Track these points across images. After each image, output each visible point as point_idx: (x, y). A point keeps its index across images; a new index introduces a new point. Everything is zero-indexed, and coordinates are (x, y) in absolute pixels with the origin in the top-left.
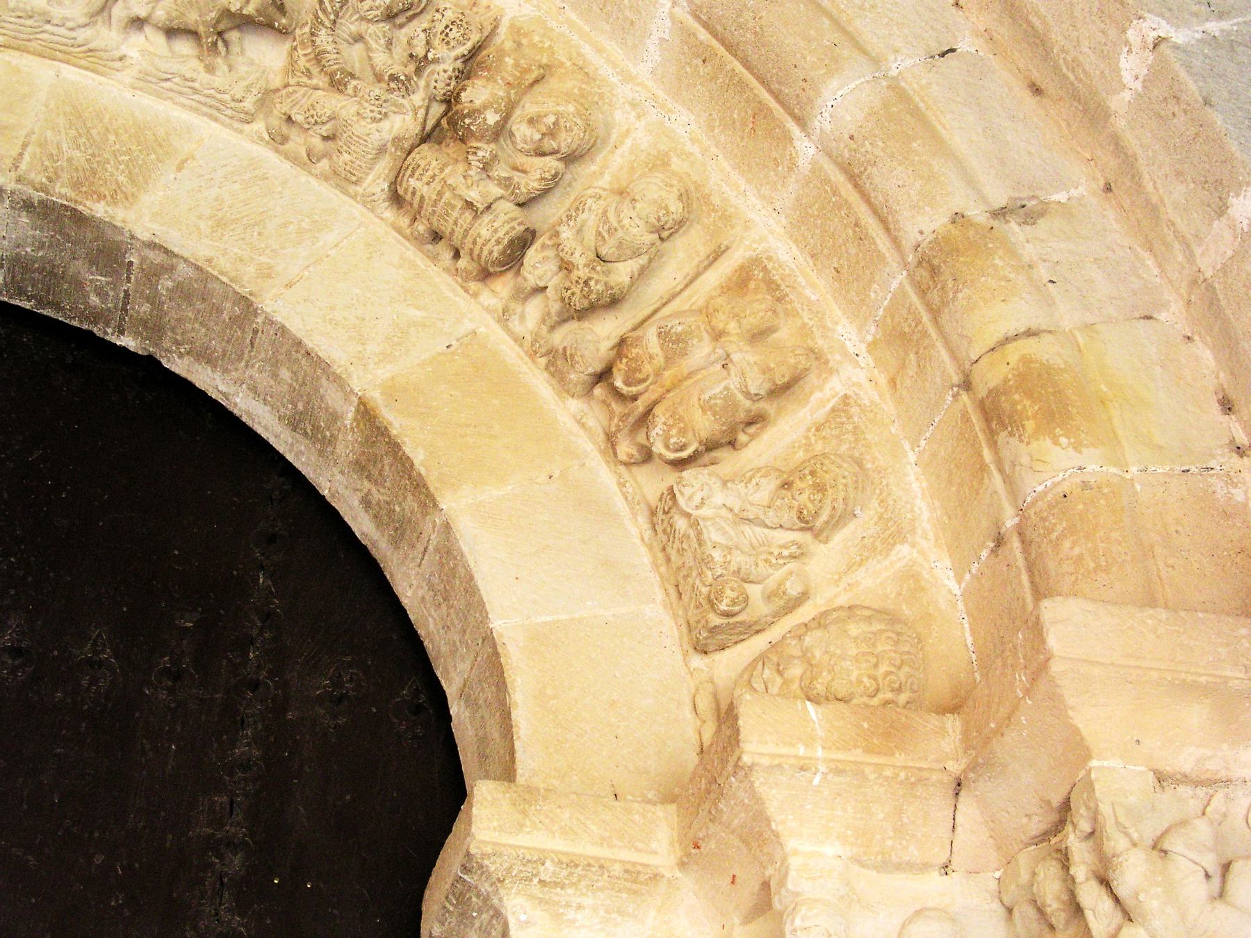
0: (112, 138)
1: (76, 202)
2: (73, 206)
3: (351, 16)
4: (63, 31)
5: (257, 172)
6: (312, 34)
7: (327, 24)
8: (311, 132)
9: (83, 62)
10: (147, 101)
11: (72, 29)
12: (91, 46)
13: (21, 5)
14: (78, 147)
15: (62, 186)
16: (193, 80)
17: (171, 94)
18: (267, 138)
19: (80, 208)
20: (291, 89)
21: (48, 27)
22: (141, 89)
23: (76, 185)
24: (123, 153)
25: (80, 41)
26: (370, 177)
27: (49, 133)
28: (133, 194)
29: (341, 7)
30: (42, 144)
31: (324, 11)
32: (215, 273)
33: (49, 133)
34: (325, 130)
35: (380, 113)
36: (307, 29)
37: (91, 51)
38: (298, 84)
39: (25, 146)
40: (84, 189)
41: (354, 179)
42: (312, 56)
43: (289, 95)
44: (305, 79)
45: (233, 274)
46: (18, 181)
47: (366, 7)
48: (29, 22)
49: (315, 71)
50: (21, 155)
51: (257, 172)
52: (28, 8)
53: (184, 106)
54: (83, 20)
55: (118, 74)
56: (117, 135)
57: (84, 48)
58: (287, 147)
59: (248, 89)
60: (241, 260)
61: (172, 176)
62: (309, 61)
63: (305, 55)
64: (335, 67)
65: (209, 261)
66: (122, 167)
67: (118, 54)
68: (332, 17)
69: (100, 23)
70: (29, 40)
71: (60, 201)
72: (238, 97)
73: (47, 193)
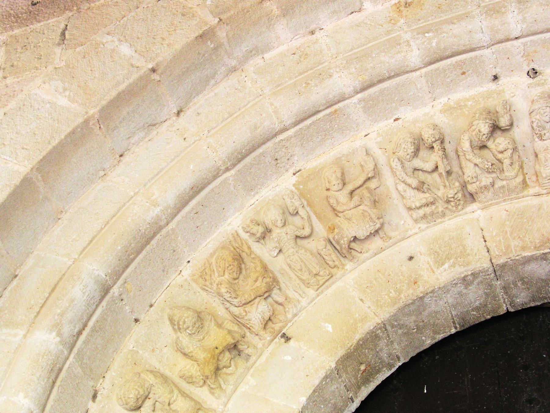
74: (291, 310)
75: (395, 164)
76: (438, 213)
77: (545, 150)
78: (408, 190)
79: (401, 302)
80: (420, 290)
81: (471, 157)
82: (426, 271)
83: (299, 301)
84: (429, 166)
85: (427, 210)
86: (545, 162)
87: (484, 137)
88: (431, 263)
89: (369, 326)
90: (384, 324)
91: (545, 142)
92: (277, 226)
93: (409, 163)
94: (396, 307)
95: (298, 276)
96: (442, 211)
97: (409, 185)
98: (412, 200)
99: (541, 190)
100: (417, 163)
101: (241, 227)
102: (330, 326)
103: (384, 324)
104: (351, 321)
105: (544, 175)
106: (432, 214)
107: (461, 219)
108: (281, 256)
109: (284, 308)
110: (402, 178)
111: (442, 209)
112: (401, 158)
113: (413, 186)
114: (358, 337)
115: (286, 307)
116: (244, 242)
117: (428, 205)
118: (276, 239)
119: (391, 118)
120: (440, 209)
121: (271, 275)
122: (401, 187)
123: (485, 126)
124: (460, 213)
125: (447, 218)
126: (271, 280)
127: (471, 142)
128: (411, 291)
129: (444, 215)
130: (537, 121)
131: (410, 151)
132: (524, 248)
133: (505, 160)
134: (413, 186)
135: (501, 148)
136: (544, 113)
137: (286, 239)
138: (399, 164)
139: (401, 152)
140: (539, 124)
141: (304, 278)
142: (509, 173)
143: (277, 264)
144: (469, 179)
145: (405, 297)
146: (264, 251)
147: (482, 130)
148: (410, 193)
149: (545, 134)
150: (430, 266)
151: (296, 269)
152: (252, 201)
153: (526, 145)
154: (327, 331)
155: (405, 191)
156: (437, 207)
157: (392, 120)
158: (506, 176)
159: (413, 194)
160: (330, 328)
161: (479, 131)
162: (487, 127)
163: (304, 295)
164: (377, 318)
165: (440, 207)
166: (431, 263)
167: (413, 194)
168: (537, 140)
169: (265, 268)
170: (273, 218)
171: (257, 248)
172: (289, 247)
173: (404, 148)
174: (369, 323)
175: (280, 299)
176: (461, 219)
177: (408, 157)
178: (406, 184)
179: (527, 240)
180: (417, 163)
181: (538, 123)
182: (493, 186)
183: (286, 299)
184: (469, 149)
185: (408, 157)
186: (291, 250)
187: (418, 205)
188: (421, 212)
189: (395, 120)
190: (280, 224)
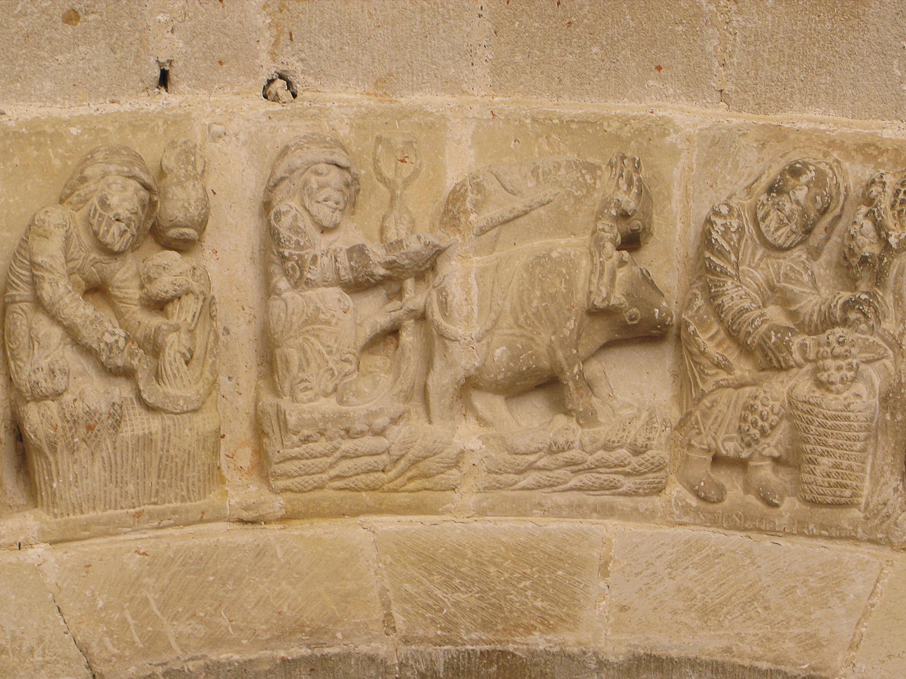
0: (492, 570)
1: (500, 642)
2: (499, 647)
3: (753, 254)
4: (368, 442)
5: (704, 553)
6: (712, 298)
7: (730, 269)
8: (752, 463)
9: (402, 498)
10: (508, 524)
11: (381, 433)
12: (410, 456)
13: (306, 416)
14: (456, 589)
15: (468, 631)
16: (569, 446)
17: (537, 495)
18: (693, 502)
19: (511, 647)
20: (706, 402)
21: (347, 445)
22: (493, 510)
23: (486, 625)
24: (519, 580)
25: (395, 451)
26: (867, 484)
27: (407, 586)
28: (568, 615)
29: (739, 240)
30: (408, 599)
31: (721, 253)
32: (747, 662)
33: (407, 586)
34: (772, 446)
35: (850, 367)
36: (699, 302)
37: (414, 463)
38: (719, 386)
39: (386, 605)
40: (500, 627)
41: (848, 493)
42: (722, 334)
43: (705, 415)
44: (723, 375)
45: (771, 655)
46: (406, 641)
47: (773, 225)
48: (321, 445)
49: (732, 355)
50: (389, 615)
51: (704, 553)
52: (317, 416)
53: (557, 511)
54: (399, 406)
55: (455, 496)
56: (495, 564)
57: (402, 463)
58: (726, 502)
59: (649, 424)
60: (769, 639)
61: (602, 584)
62: (718, 345)
63: (712, 338)
64: (765, 326)
65: (728, 650)
66: (529, 593)
67: (452, 451)
68: (733, 258)
69: (414, 416)
70: (321, 488)
71: (478, 648)
72: (641, 441)
73: (455, 644)
77: (306, 323)
81: (62, 290)
86: (301, 368)
87: (115, 229)
91: (309, 293)
99: (267, 496)
105: (292, 420)
123: (124, 188)
127: (67, 239)
130: (293, 212)
132: (216, 642)
133: (172, 337)
135: (164, 285)
136: (321, 187)
140: (300, 224)
142: (180, 388)
144: (40, 376)
147: (114, 200)
149: (315, 259)
153: (233, 329)
158: (166, 395)
161: (104, 203)
162: (130, 193)
168: (283, 284)
179: (227, 623)
181: (295, 218)
182: (117, 425)
184: (59, 263)
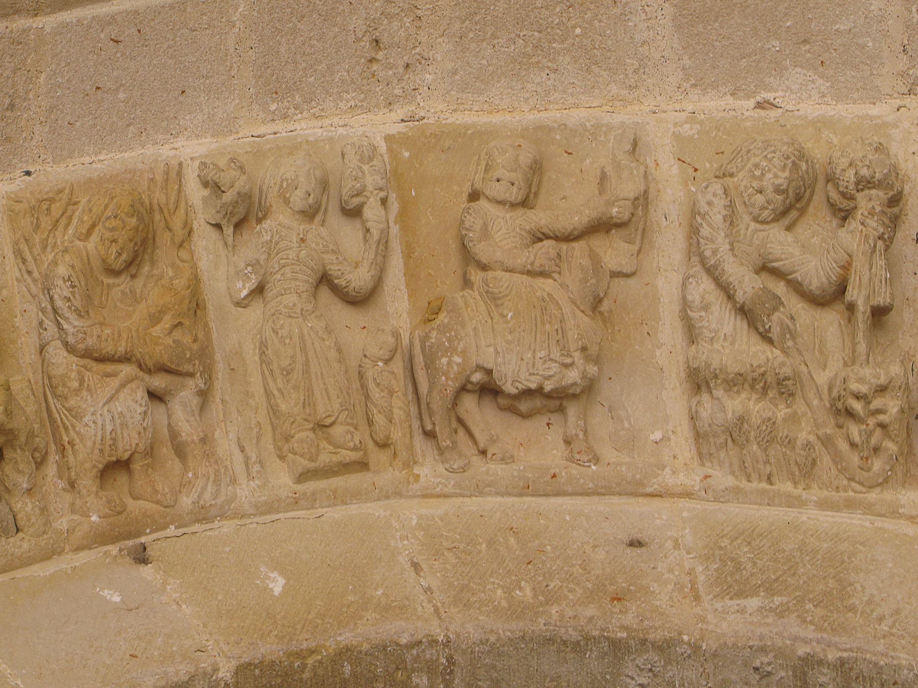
74: (199, 484)
75: (710, 197)
76: (791, 443)
78: (715, 308)
79: (541, 621)
80: (624, 620)
82: (670, 587)
83: (234, 481)
84: (816, 272)
85: (755, 407)
88: (702, 578)
89: (402, 630)
90: (450, 659)
92: (287, 202)
93: (753, 225)
94: (516, 627)
95: (268, 394)
96: (808, 445)
97: (727, 290)
98: (717, 346)
100: (781, 243)
101: (197, 163)
102: (281, 581)
103: (450, 659)
104: (351, 598)
106: (769, 436)
107: (867, 524)
108: (255, 312)
109: (186, 469)
110: (715, 252)
111: (812, 438)
112: (733, 192)
113: (740, 297)
114: (346, 637)
115: (191, 464)
116: (182, 211)
117: (765, 391)
118: (267, 237)
119: (748, 97)
120: (804, 434)
121: (201, 336)
122: (702, 288)
124: (873, 496)
125: (815, 493)
126: (195, 347)
128: (591, 611)
129: (807, 471)
131: (768, 181)
134: (740, 297)
137: (292, 254)
138: (720, 203)
139: (741, 175)
141: (283, 407)
143: (237, 333)
145: (562, 616)
146: (219, 265)
148: (720, 320)
150: (693, 583)
151: (275, 366)
152: (262, 130)
154: (266, 588)
155: (706, 308)
156: (793, 419)
157: (751, 103)
159: (728, 328)
160: (277, 585)
163: (257, 468)
164: (435, 622)
165: (807, 423)
166: (702, 578)
167: (728, 328)
169: (196, 306)
170: (290, 175)
171: (205, 242)
172: (291, 289)
173: (757, 166)
174: (403, 624)
175: (187, 428)
176: (867, 524)
177: (760, 199)
178: (717, 281)
180: (781, 243)
183: (203, 441)
185: (760, 199)
186: (291, 299)
187: (734, 367)
188: (735, 404)
189: (759, 105)
190: (298, 199)
